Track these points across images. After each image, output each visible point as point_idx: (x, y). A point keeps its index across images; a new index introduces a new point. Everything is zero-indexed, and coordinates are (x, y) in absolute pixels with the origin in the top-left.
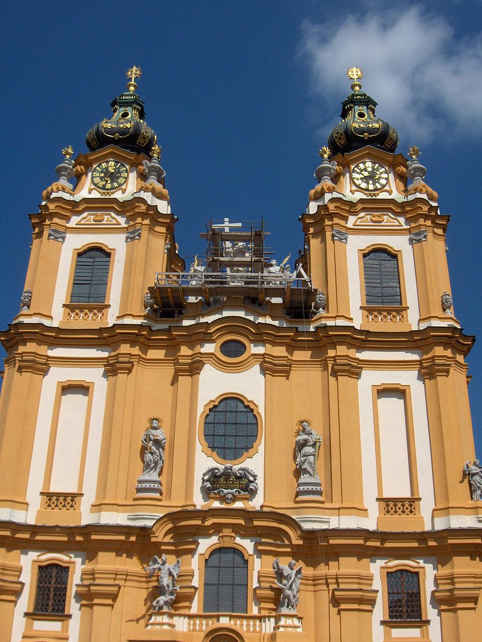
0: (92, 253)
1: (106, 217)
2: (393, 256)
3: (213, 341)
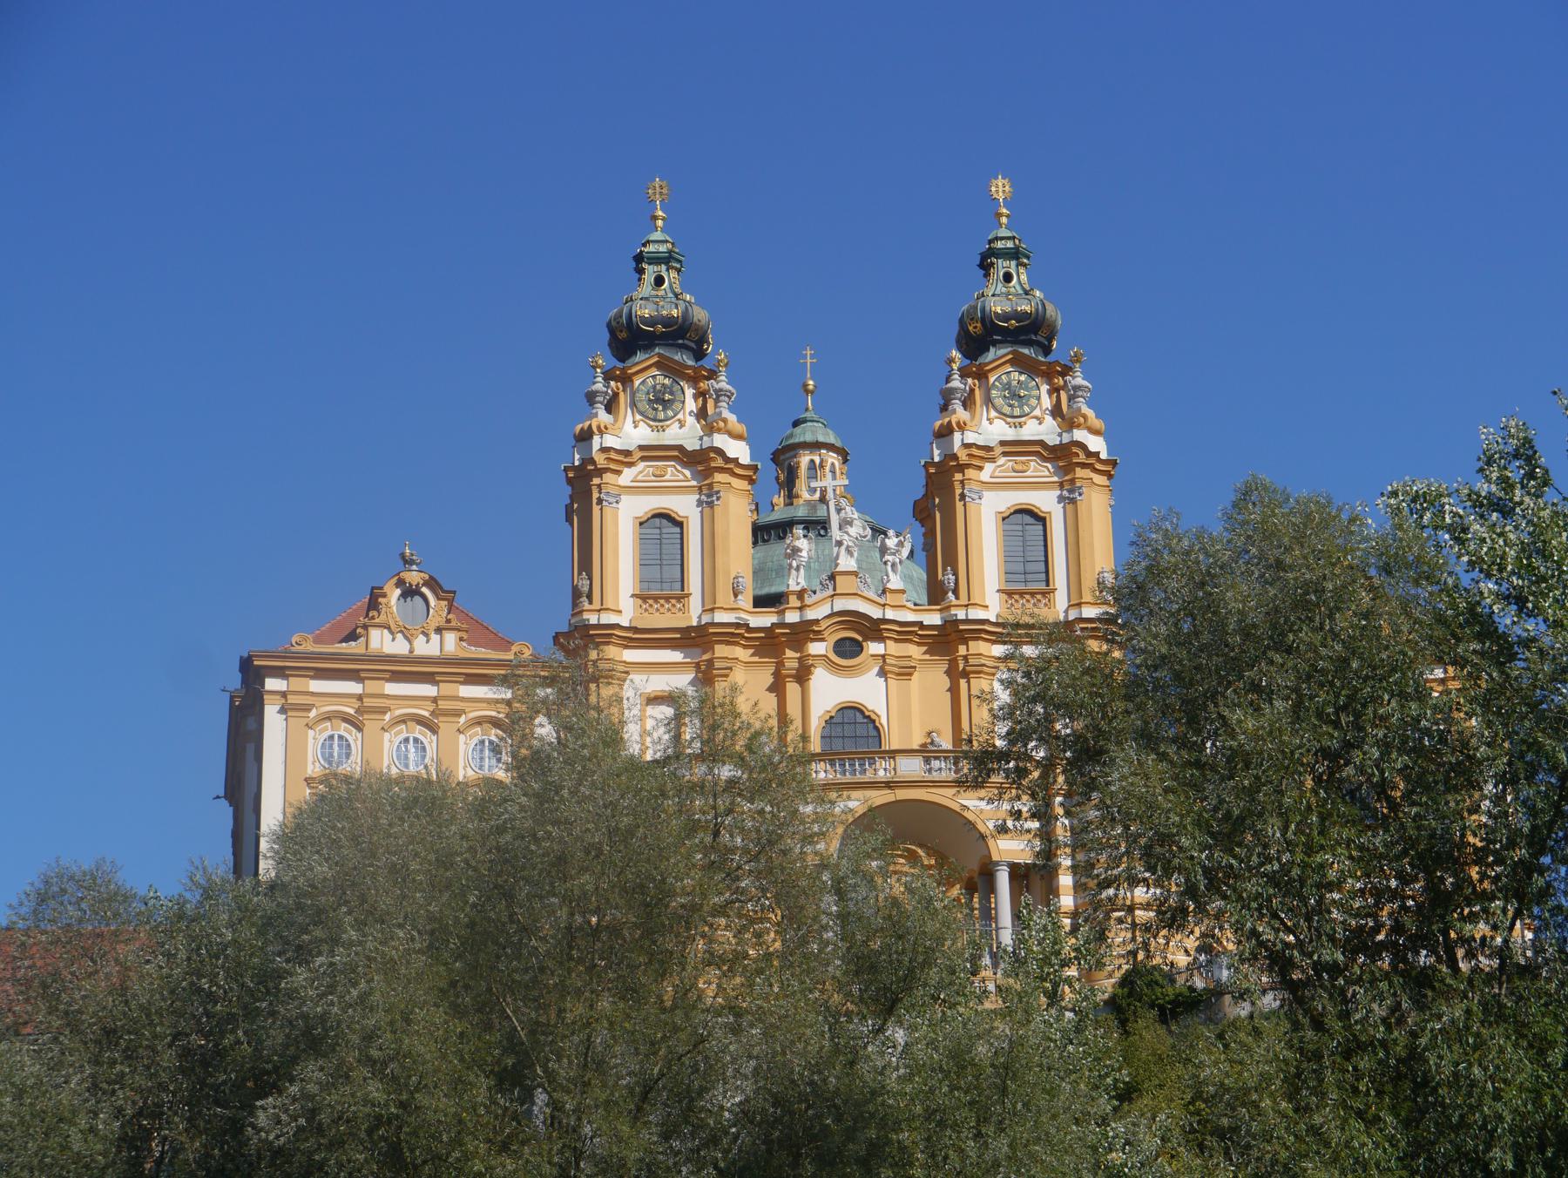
0: (657, 520)
1: (669, 469)
2: (1041, 519)
3: (823, 640)
